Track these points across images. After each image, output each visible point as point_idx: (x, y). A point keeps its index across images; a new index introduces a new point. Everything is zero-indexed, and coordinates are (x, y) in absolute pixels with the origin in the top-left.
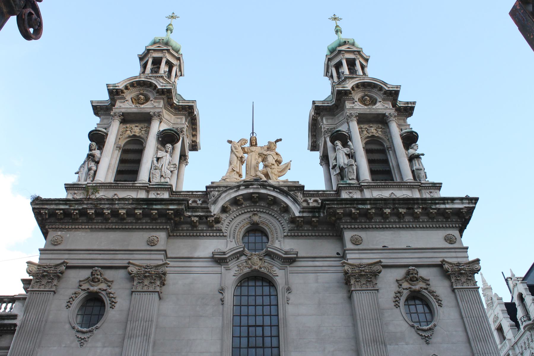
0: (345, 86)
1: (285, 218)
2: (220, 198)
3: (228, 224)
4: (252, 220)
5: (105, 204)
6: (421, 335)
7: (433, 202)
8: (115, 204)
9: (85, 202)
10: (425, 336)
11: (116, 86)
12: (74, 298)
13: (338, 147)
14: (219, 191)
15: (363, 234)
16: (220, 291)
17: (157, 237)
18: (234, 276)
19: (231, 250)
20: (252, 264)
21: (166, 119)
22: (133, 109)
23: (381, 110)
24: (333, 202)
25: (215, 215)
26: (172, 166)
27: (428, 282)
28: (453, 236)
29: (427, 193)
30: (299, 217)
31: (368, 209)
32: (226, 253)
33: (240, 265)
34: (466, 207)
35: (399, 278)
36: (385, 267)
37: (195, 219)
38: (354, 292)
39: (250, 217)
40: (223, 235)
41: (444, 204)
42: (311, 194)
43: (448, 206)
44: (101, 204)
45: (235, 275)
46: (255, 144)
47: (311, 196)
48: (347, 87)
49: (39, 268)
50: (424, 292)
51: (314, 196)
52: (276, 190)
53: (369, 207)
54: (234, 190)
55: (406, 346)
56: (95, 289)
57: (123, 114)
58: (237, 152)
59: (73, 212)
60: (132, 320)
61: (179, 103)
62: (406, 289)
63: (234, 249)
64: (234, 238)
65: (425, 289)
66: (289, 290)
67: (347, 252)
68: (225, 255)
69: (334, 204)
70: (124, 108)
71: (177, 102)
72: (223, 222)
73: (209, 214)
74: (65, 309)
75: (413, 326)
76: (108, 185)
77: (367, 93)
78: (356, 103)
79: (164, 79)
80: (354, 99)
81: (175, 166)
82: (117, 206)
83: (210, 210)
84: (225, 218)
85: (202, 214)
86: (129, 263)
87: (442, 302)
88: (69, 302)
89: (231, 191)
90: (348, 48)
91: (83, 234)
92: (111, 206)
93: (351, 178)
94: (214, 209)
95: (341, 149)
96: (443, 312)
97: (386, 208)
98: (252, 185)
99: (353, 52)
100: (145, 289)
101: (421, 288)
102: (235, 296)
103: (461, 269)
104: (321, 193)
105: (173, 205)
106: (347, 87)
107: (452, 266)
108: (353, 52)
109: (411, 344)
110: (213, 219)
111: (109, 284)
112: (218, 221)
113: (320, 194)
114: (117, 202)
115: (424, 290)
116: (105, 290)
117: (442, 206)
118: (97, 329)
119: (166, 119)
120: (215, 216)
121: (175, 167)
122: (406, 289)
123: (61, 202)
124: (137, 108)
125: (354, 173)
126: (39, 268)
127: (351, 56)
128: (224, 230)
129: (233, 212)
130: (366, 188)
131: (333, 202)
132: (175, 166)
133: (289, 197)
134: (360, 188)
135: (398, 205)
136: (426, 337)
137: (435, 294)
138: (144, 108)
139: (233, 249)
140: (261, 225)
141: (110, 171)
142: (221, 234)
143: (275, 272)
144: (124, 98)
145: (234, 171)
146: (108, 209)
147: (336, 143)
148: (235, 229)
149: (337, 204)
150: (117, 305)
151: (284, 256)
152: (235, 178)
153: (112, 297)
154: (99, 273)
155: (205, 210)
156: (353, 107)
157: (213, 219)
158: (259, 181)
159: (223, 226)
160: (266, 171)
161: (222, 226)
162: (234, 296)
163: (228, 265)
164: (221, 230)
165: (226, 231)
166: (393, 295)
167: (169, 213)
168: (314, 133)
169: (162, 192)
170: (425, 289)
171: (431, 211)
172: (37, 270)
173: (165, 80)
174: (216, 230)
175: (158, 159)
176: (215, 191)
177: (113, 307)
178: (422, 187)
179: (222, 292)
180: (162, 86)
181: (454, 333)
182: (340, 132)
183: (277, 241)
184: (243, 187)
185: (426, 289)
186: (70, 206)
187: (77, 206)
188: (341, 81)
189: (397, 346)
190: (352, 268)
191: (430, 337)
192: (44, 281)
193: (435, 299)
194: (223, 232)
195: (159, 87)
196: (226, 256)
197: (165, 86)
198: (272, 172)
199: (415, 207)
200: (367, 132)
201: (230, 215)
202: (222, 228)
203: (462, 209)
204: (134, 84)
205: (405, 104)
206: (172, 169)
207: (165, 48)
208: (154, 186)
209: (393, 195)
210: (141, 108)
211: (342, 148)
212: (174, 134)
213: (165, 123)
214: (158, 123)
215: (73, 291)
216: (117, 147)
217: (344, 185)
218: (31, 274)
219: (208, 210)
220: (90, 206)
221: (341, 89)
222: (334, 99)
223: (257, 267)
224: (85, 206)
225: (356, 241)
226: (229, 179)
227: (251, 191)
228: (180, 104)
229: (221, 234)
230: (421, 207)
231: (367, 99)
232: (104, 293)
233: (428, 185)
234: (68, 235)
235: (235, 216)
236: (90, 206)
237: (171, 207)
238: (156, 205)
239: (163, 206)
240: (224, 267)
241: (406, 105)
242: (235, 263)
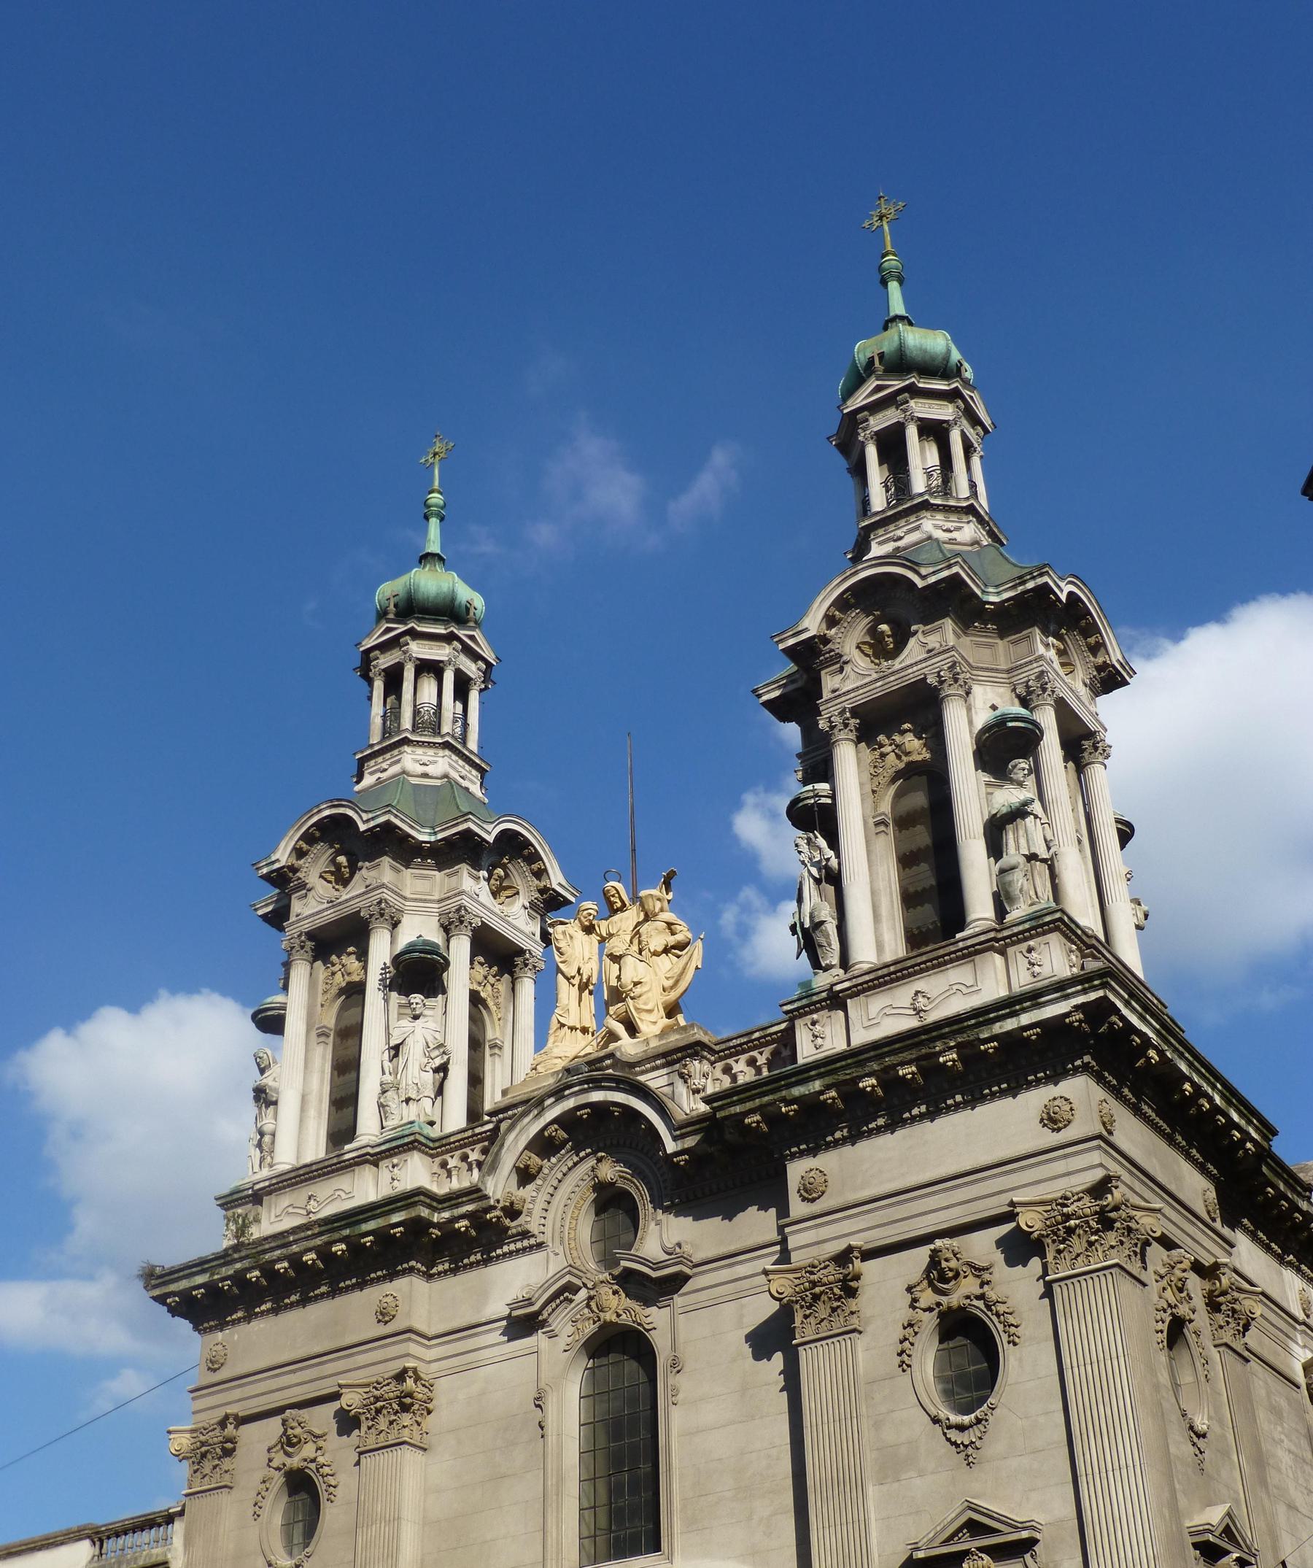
0: (800, 629)
5: (272, 1249)
6: (955, 1444)
7: (981, 1019)
8: (289, 1244)
9: (236, 1256)
10: (962, 1443)
11: (273, 863)
12: (263, 1493)
15: (828, 1161)
16: (537, 1403)
17: (395, 1295)
18: (565, 1351)
19: (542, 1289)
20: (598, 1308)
21: (415, 900)
22: (326, 913)
23: (915, 669)
24: (729, 1100)
26: (436, 1053)
27: (986, 1276)
28: (1066, 1100)
29: (1018, 954)
30: (677, 1154)
31: (821, 1093)
32: (533, 1300)
33: (578, 1316)
34: (1077, 1008)
35: (912, 1282)
36: (868, 1255)
37: (462, 1225)
38: (800, 1349)
39: (593, 1169)
41: (1014, 1014)
42: (734, 1047)
43: (1025, 1019)
44: (265, 1252)
45: (567, 1348)
46: (619, 904)
47: (737, 1054)
48: (806, 630)
49: (195, 1435)
50: (977, 1308)
51: (744, 1052)
53: (817, 1085)
54: (531, 1116)
55: (918, 1481)
56: (295, 1462)
57: (311, 935)
59: (223, 1286)
60: (365, 1525)
61: (435, 833)
62: (930, 1309)
63: (550, 1282)
64: (562, 1242)
65: (978, 1298)
66: (676, 1366)
67: (787, 1230)
68: (532, 1304)
69: (733, 1104)
70: (307, 917)
71: (430, 834)
72: (531, 1206)
73: (483, 1204)
74: (254, 1523)
75: (936, 1420)
76: (293, 1174)
79: (413, 741)
81: (442, 1050)
82: (295, 1248)
84: (534, 1194)
85: (470, 1207)
86: (340, 1386)
87: (1019, 1331)
88: (256, 1504)
89: (526, 1120)
90: (879, 389)
91: (261, 1326)
92: (284, 1251)
94: (496, 1186)
96: (1020, 1360)
97: (861, 1078)
100: (382, 1440)
101: (968, 1297)
102: (583, 1397)
103: (1067, 1217)
104: (757, 1035)
105: (398, 1211)
107: (1049, 1208)
109: (932, 1473)
111: (321, 1443)
112: (513, 1212)
113: (755, 1040)
114: (291, 1238)
115: (975, 1302)
116: (313, 1461)
117: (1010, 1025)
118: (309, 1557)
119: (415, 900)
121: (444, 1053)
122: (930, 1309)
123: (194, 1270)
124: (333, 906)
125: (830, 945)
126: (195, 1435)
128: (533, 1228)
130: (851, 997)
131: (729, 1100)
132: (442, 1050)
133: (650, 1099)
135: (892, 1058)
136: (966, 1446)
137: (1001, 1308)
138: (347, 901)
139: (546, 1285)
141: (312, 1112)
142: (532, 1241)
143: (649, 1320)
144: (303, 886)
145: (563, 1025)
146: (279, 1260)
149: (741, 1101)
150: (338, 1491)
151: (654, 1274)
152: (556, 1058)
153: (327, 1475)
154: (295, 1424)
155: (475, 1196)
159: (531, 1222)
161: (529, 1219)
162: (580, 1398)
163: (550, 1326)
166: (900, 1333)
167: (395, 1234)
169: (403, 1156)
170: (978, 1298)
171: (982, 1047)
172: (193, 1440)
173: (418, 742)
174: (518, 1234)
175: (396, 1050)
177: (332, 1497)
178: (1004, 939)
179: (540, 1403)
180: (368, 821)
181: (1042, 1420)
182: (801, 804)
183: (652, 1224)
184: (552, 1100)
185: (981, 1297)
186: (212, 1275)
187: (224, 1269)
189: (896, 1485)
190: (799, 1278)
191: (978, 1444)
192: (207, 1466)
193: (1000, 1322)
195: (362, 827)
196: (536, 1308)
197: (373, 819)
198: (637, 1009)
199: (937, 1048)
201: (544, 1180)
202: (529, 1227)
203: (1067, 1015)
204: (301, 848)
205: (1014, 587)
206: (438, 1062)
207: (402, 628)
208: (383, 1148)
209: (920, 999)
210: (340, 904)
212: (421, 957)
213: (415, 912)
214: (387, 935)
215: (259, 1476)
216: (319, 1035)
217: (796, 1005)
218: (181, 1457)
219: (479, 1194)
220: (246, 1263)
221: (791, 642)
223: (609, 1316)
224: (238, 1266)
225: (809, 1194)
226: (542, 1065)
227: (570, 1103)
228: (440, 836)
229: (532, 1241)
230: (952, 1044)
232: (313, 1466)
233: (1021, 928)
234: (236, 1337)
236: (246, 1263)
237: (396, 1218)
238: (366, 1220)
239: (379, 1220)
240: (544, 1333)
241: (1020, 589)
242: (565, 1316)
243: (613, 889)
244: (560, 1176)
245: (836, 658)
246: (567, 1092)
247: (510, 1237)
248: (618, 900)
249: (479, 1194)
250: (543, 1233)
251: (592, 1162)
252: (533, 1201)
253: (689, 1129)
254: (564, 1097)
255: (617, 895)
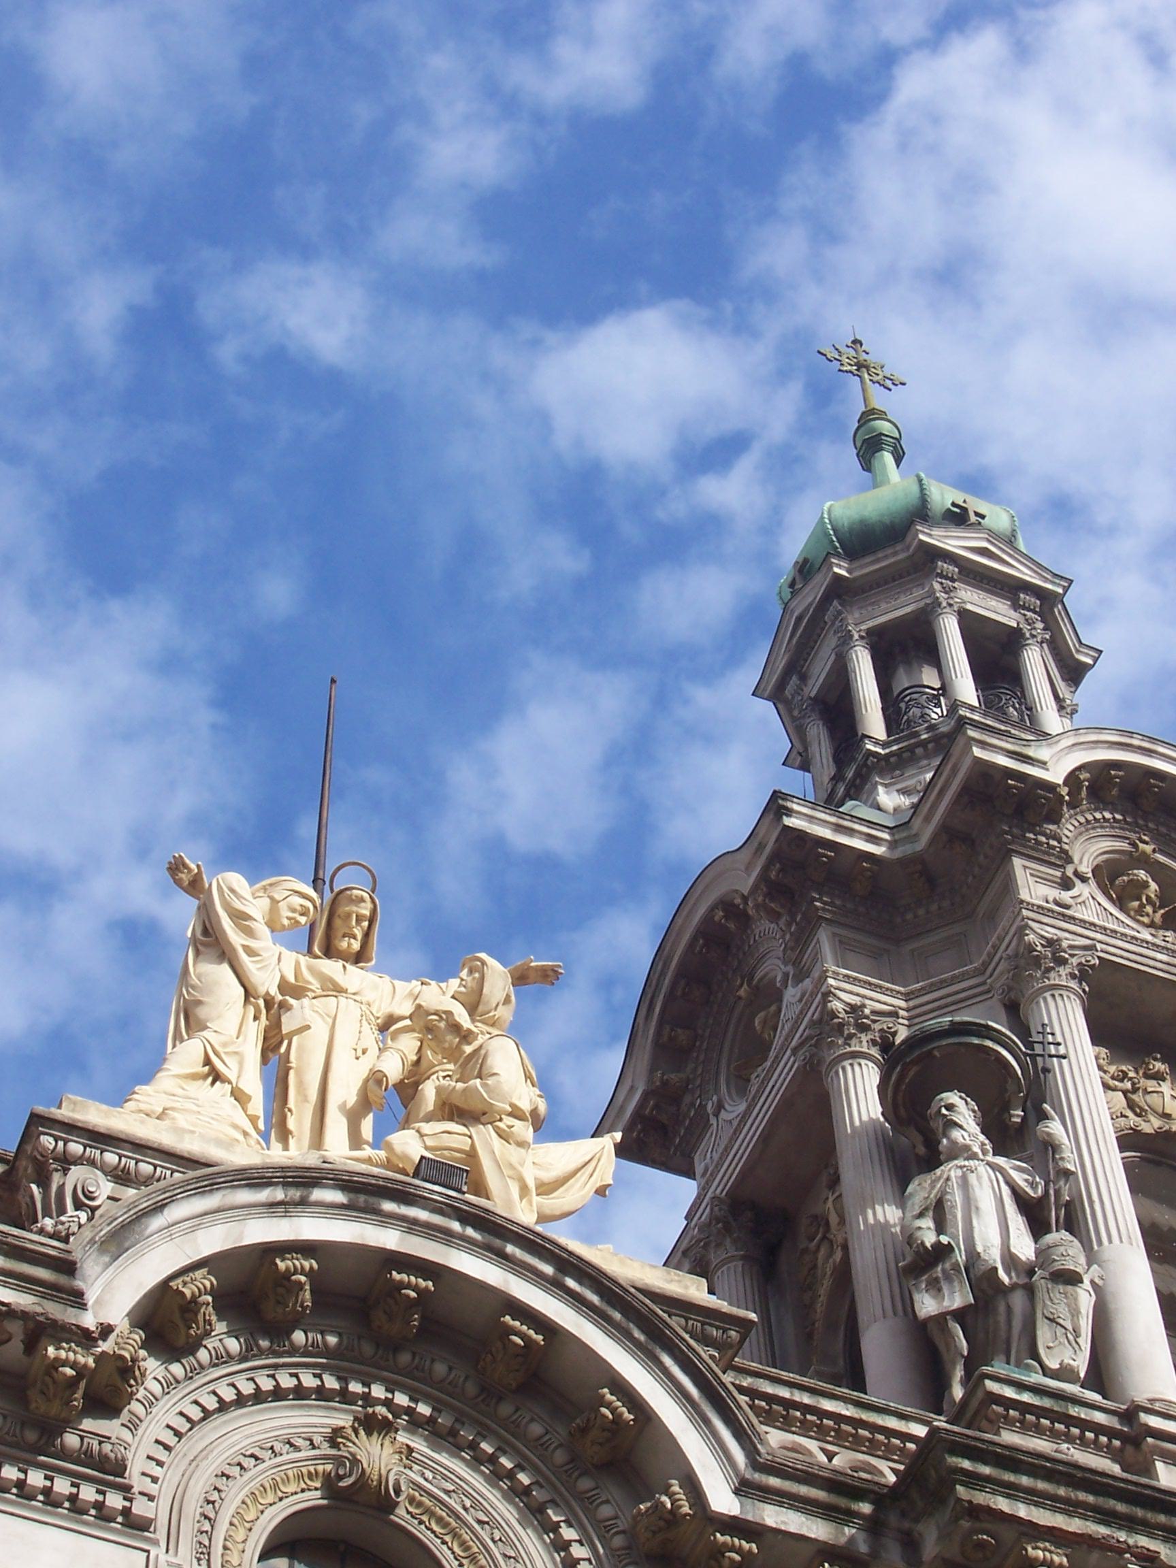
0: (1030, 752)
1: (606, 1511)
2: (157, 1222)
3: (170, 1439)
4: (355, 1461)
13: (956, 1134)
14: (121, 1177)
25: (106, 1330)
30: (734, 1525)
39: (335, 1437)
40: (126, 1512)
46: (356, 946)
52: (571, 1283)
54: (264, 1195)
58: (250, 952)
73: (56, 1311)
77: (1148, 848)
78: (1080, 888)
80: (1069, 860)
83: (79, 1284)
93: (1053, 1364)
95: (976, 1149)
98: (404, 1196)
99: (1009, 588)
106: (1043, 764)
108: (1009, 588)
110: (91, 1362)
120: (105, 1346)
127: (998, 610)
129: (221, 1359)
134: (1130, 1449)
140: (401, 1516)
142: (115, 1501)
147: (950, 1107)
148: (215, 1496)
156: (1068, 907)
157: (91, 1362)
158: (455, 1181)
160: (465, 1144)
161: (126, 1435)
164: (119, 1468)
165: (153, 1489)
168: (682, 1036)
174: (86, 1457)
176: (92, 1163)
184: (338, 1197)
188: (924, 744)
194: (126, 1489)
200: (1131, 1105)
211: (985, 1153)
221: (1003, 761)
222: (927, 819)
227: (389, 1239)
229: (115, 1501)
231: (1145, 885)
235: (211, 1403)
243: (369, 905)
244: (229, 1395)
245: (1059, 858)
246: (388, 1206)
247: (64, 1454)
248: (359, 933)
249: (62, 1280)
250: (151, 1498)
251: (343, 1419)
252: (149, 1404)
253: (803, 1490)
254: (377, 1212)
255: (366, 924)
